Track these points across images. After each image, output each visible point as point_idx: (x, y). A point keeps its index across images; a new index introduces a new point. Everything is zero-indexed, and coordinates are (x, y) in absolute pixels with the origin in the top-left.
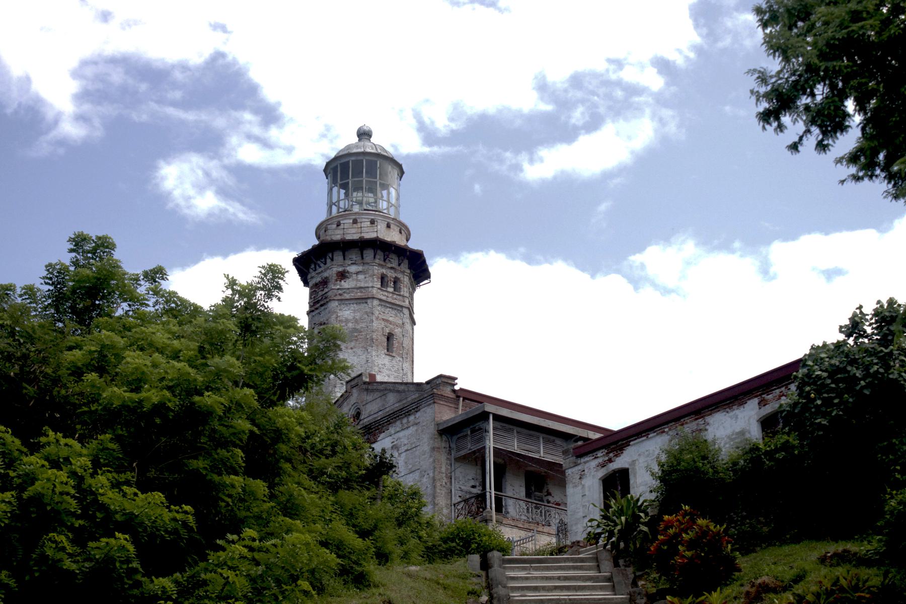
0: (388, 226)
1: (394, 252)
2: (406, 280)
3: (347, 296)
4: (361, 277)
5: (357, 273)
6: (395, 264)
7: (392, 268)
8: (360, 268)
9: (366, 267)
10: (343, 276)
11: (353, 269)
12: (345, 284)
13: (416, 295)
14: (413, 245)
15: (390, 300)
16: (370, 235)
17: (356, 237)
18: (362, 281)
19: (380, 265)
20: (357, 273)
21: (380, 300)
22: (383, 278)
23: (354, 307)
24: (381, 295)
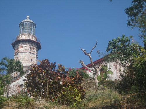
0: (32, 37)
1: (33, 42)
2: (35, 48)
3: (23, 52)
4: (26, 47)
5: (25, 47)
6: (33, 45)
7: (32, 46)
8: (26, 46)
9: (27, 45)
10: (22, 47)
11: (24, 46)
12: (22, 49)
13: (38, 52)
14: (37, 41)
15: (32, 52)
16: (27, 38)
17: (25, 39)
18: (26, 48)
19: (30, 45)
20: (25, 47)
21: (30, 52)
22: (30, 48)
23: (24, 54)
24: (30, 51)
